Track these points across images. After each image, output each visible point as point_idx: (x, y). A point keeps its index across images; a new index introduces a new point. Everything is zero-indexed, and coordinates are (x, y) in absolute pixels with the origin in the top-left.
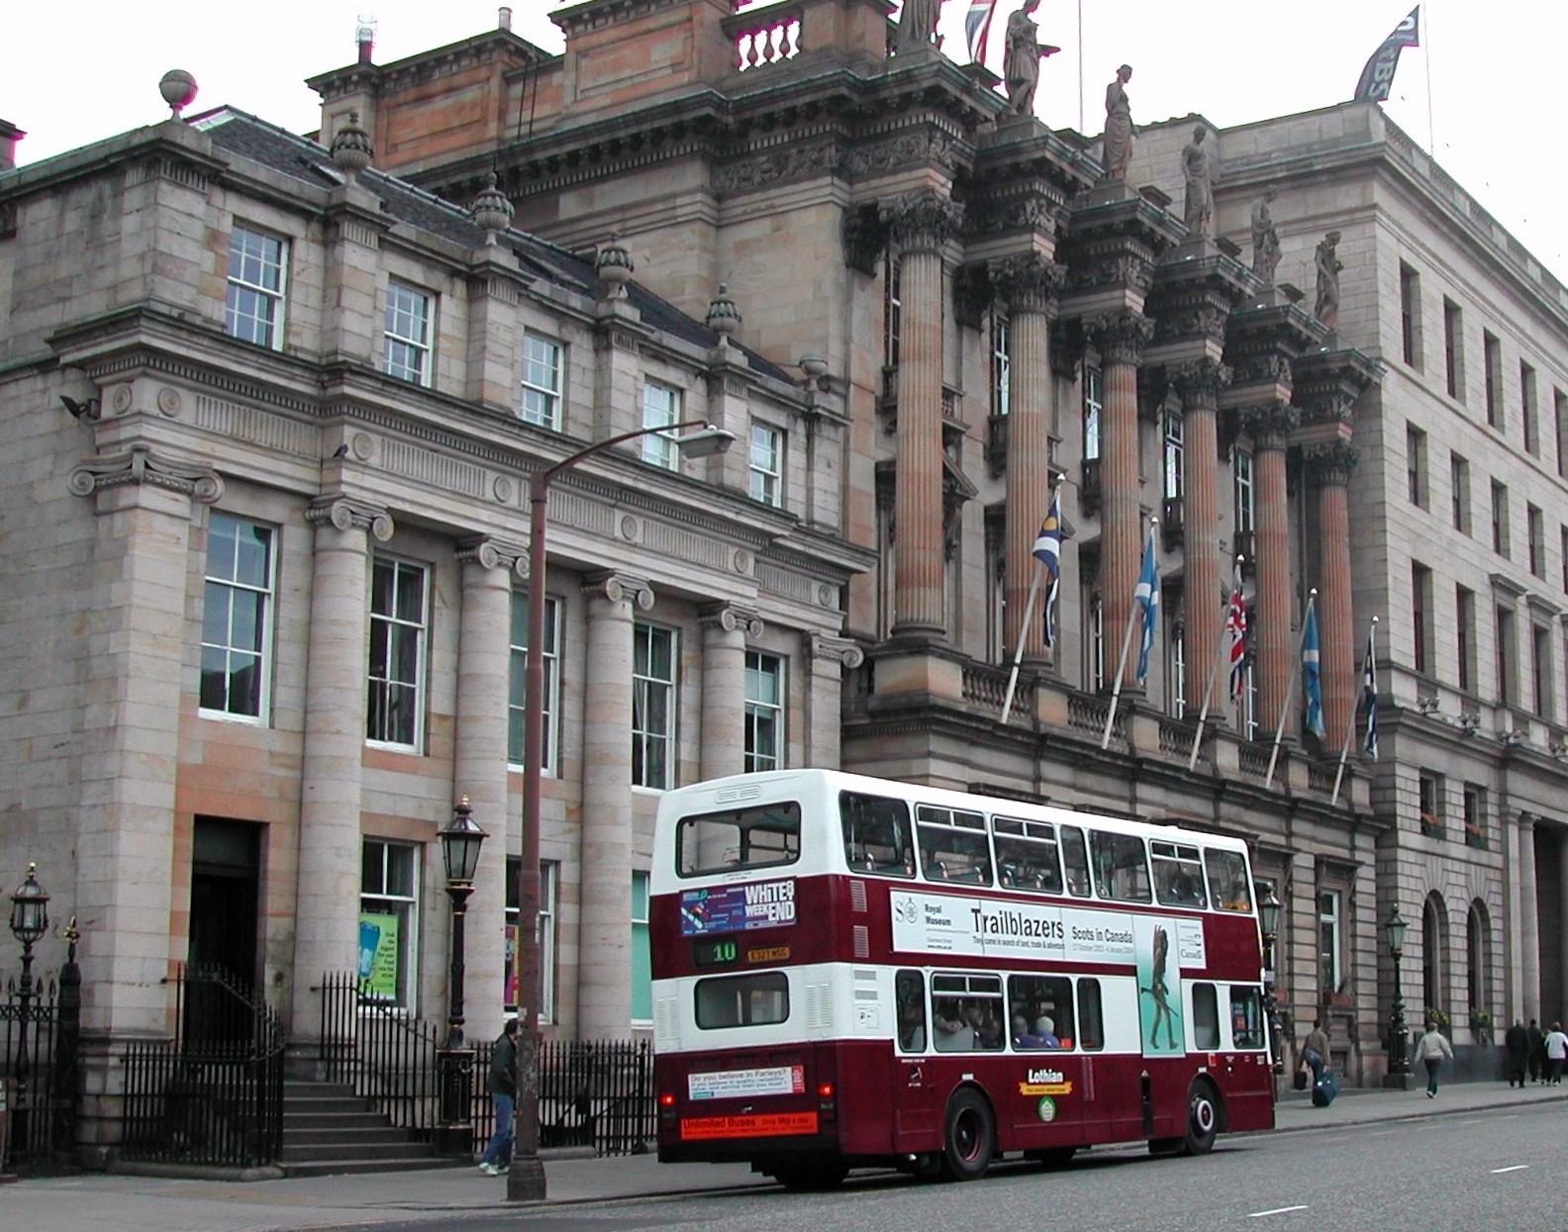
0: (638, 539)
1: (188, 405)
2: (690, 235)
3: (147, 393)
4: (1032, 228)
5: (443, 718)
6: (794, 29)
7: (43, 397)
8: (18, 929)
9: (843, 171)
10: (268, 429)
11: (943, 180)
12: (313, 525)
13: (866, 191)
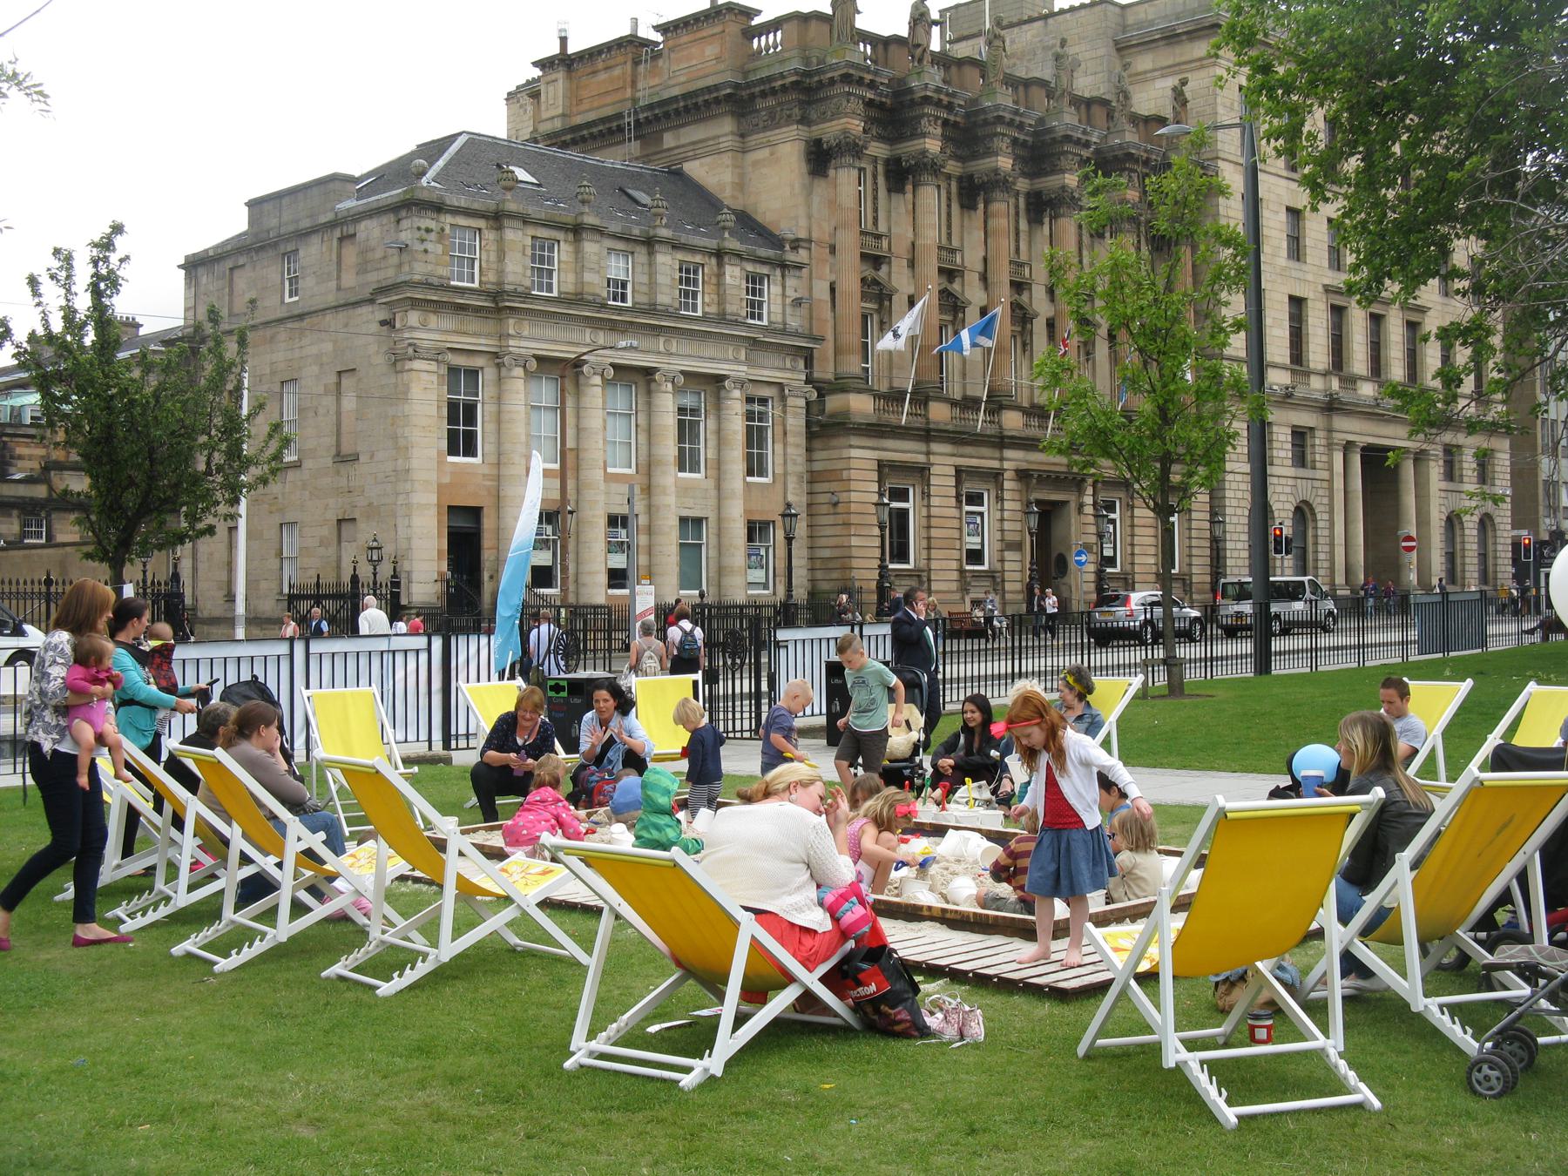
0: (674, 350)
1: (433, 320)
2: (727, 159)
3: (414, 317)
4: (924, 135)
5: (571, 450)
6: (779, 34)
7: (369, 317)
8: (371, 561)
9: (804, 121)
10: (473, 324)
11: (857, 122)
12: (499, 366)
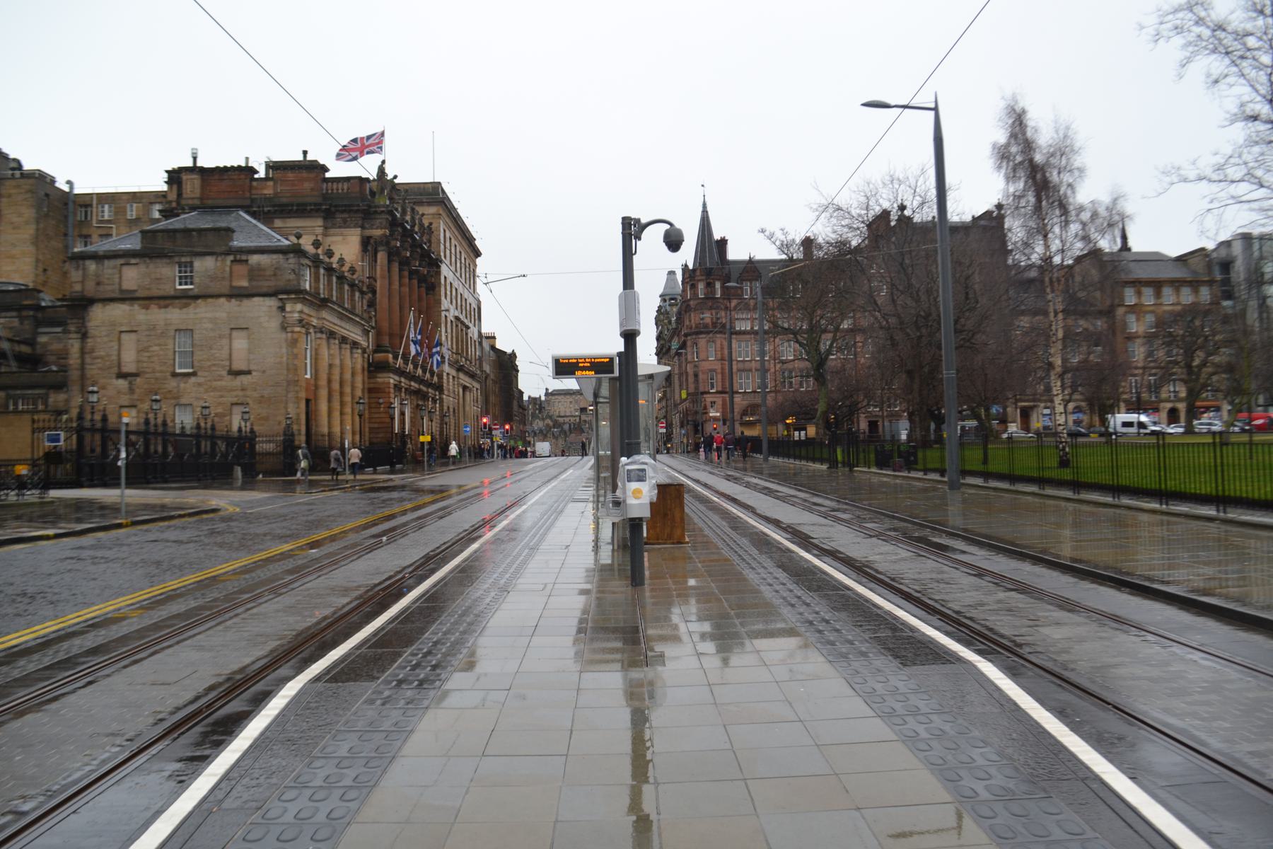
9: (363, 227)
13: (368, 232)
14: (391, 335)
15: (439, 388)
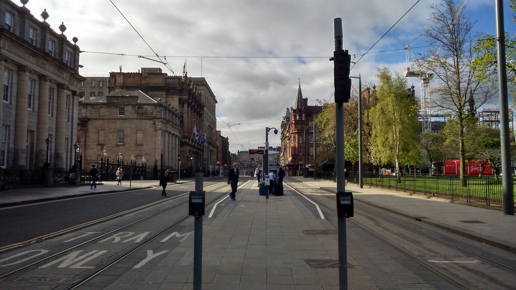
14: (188, 132)
15: (202, 151)
